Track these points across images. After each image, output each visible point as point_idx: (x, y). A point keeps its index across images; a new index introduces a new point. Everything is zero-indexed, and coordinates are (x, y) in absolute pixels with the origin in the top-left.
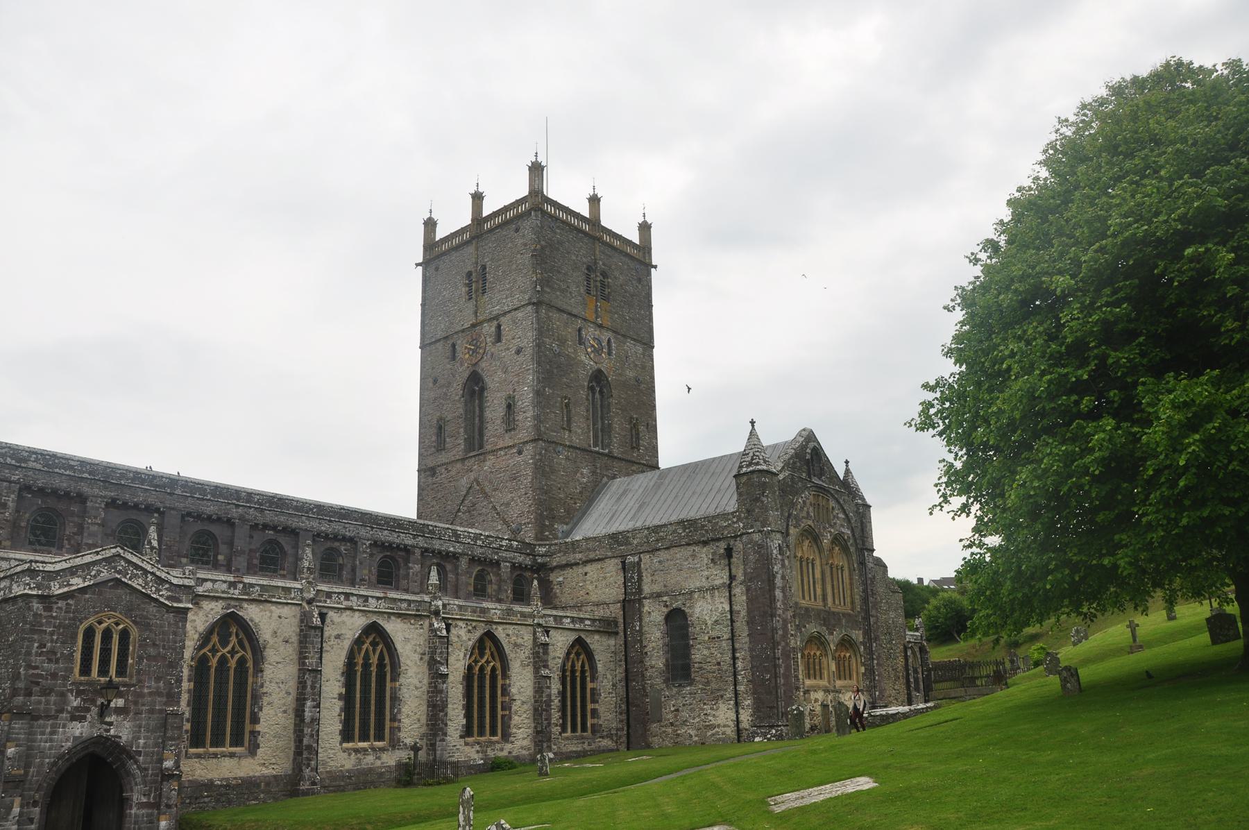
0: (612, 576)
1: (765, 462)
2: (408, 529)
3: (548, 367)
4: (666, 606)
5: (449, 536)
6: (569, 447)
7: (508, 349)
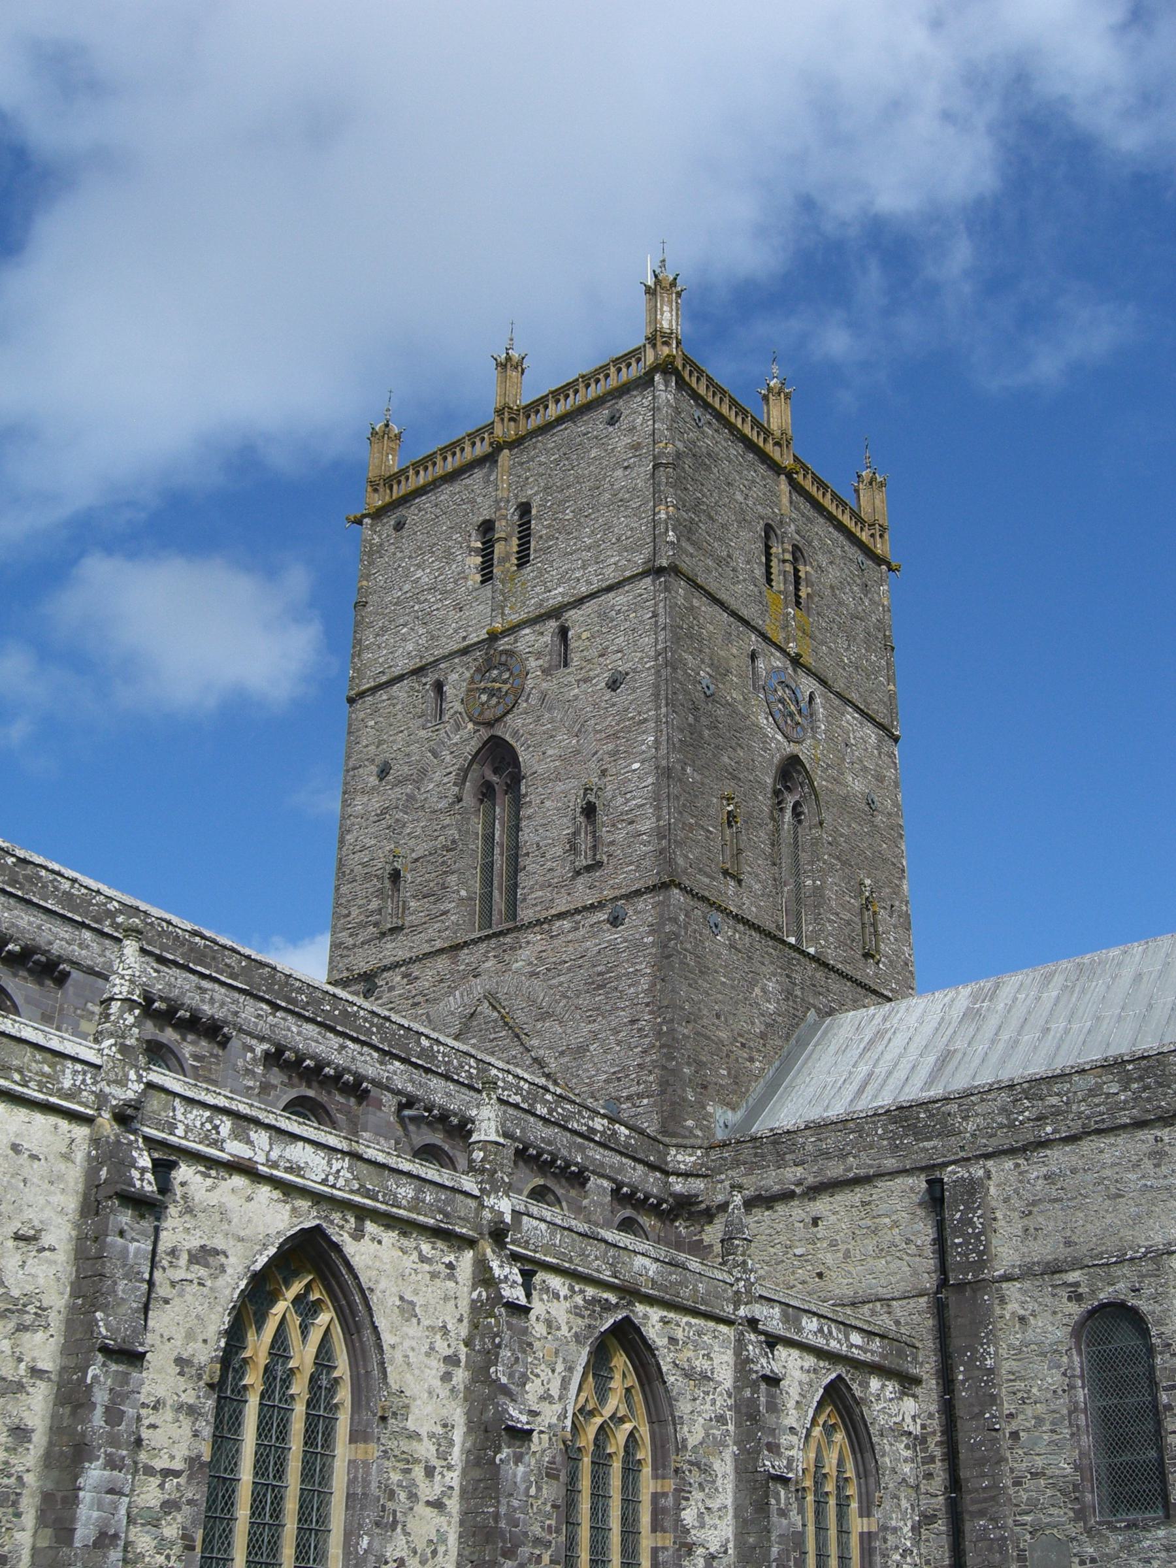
0: (896, 1224)
2: (368, 1032)
3: (691, 719)
4: (1077, 1298)
5: (470, 1076)
7: (586, 680)
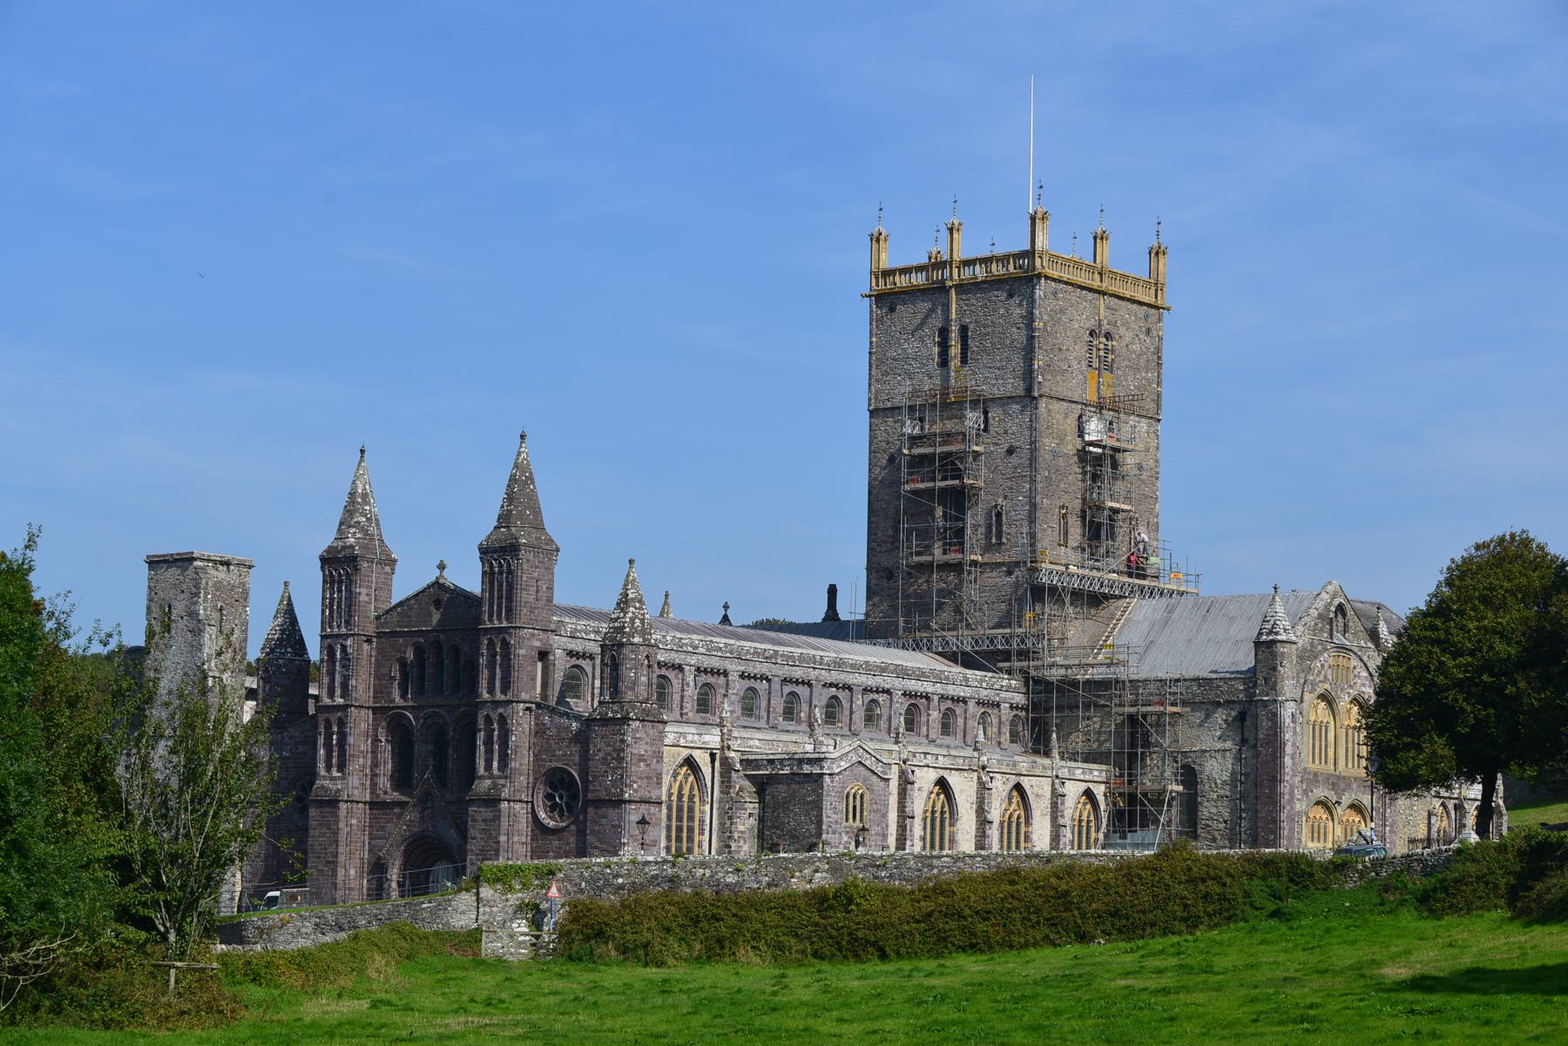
1: (1285, 630)
2: (929, 677)
3: (1047, 474)
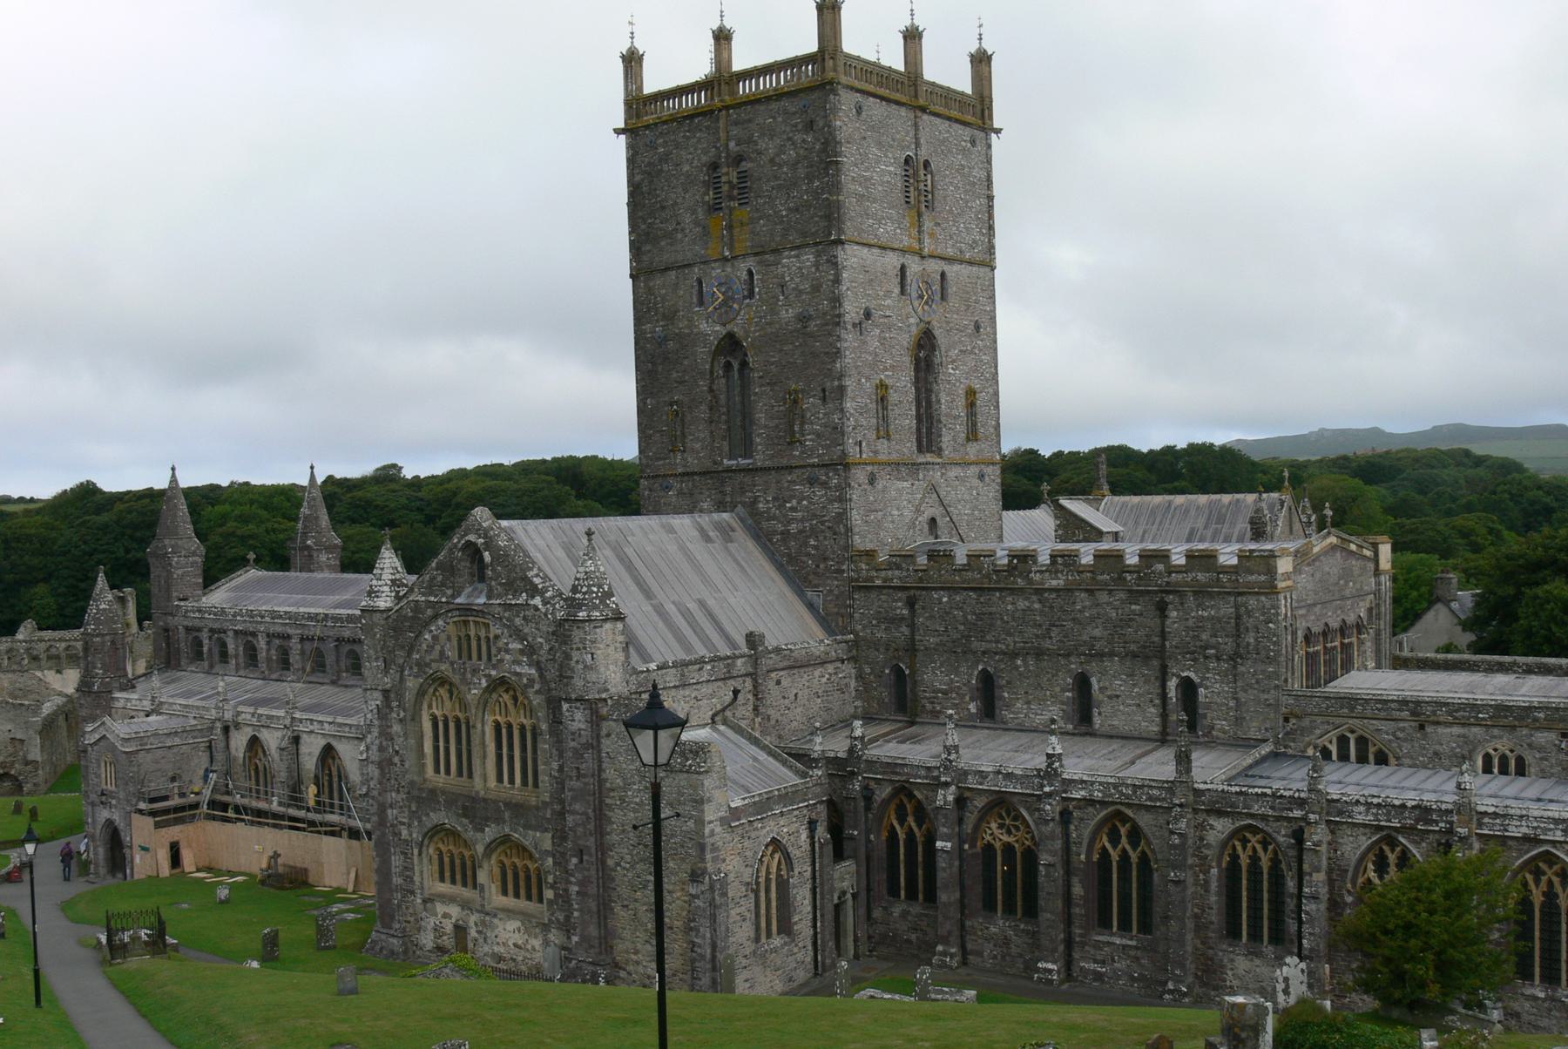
6: (683, 474)
